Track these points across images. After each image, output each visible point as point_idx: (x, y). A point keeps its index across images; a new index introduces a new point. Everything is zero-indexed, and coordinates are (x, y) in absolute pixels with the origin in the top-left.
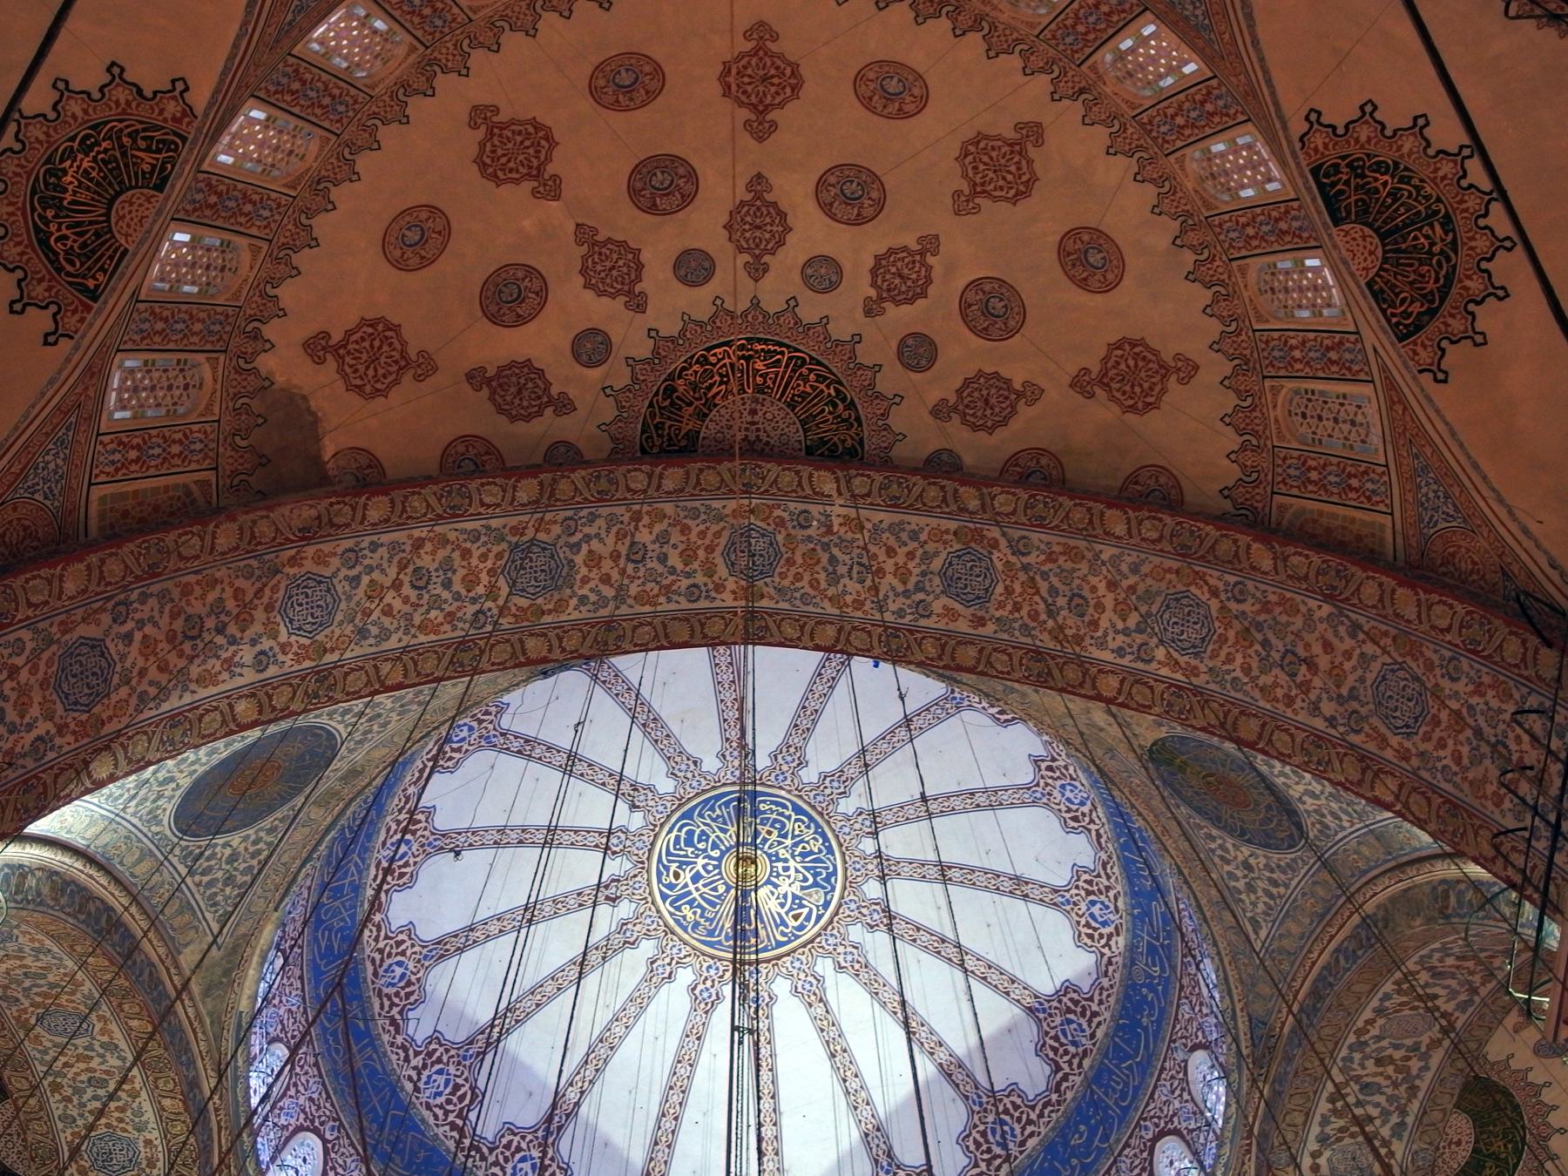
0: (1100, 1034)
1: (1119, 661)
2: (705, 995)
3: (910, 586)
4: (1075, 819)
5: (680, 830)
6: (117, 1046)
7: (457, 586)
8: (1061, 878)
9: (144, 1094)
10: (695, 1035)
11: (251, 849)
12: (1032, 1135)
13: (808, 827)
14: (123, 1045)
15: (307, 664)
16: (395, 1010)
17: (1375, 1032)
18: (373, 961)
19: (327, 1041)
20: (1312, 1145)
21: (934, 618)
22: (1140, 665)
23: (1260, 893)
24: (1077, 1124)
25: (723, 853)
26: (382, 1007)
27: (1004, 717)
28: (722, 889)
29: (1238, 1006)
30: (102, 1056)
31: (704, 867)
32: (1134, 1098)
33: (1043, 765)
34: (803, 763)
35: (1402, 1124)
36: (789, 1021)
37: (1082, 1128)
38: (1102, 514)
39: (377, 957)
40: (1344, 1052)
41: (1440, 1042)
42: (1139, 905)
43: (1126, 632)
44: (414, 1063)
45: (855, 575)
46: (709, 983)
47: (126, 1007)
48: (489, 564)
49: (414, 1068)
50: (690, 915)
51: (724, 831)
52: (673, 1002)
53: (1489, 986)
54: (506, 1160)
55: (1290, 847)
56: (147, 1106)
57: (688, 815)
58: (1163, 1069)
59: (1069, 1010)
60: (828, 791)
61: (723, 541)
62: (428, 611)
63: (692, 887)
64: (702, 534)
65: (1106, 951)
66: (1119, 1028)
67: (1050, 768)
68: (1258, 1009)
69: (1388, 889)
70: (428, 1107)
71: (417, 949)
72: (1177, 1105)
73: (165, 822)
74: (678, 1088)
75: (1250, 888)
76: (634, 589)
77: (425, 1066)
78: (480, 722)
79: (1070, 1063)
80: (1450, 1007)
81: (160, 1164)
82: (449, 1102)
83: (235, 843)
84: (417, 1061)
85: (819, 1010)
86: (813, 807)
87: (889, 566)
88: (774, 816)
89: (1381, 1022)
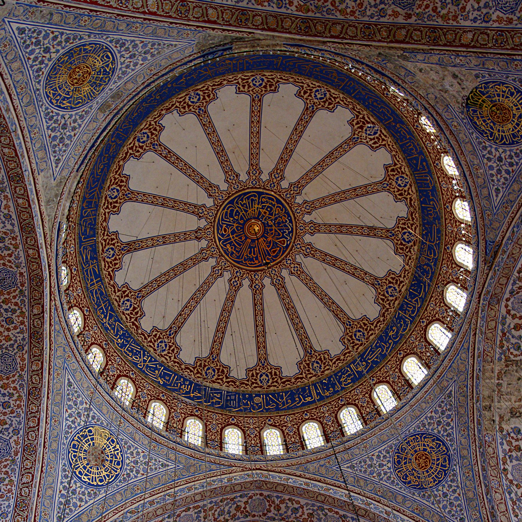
2: (235, 284)
5: (228, 209)
10: (231, 300)
13: (282, 210)
16: (110, 270)
18: (102, 244)
19: (84, 274)
25: (245, 222)
26: (105, 266)
28: (243, 238)
31: (237, 227)
36: (270, 294)
39: (104, 243)
44: (117, 294)
46: (237, 279)
49: (118, 296)
54: (155, 341)
57: (231, 202)
60: (292, 192)
63: (231, 236)
70: (123, 313)
71: (119, 244)
73: (42, 83)
77: (122, 297)
82: (132, 313)
86: (285, 200)
88: (268, 205)
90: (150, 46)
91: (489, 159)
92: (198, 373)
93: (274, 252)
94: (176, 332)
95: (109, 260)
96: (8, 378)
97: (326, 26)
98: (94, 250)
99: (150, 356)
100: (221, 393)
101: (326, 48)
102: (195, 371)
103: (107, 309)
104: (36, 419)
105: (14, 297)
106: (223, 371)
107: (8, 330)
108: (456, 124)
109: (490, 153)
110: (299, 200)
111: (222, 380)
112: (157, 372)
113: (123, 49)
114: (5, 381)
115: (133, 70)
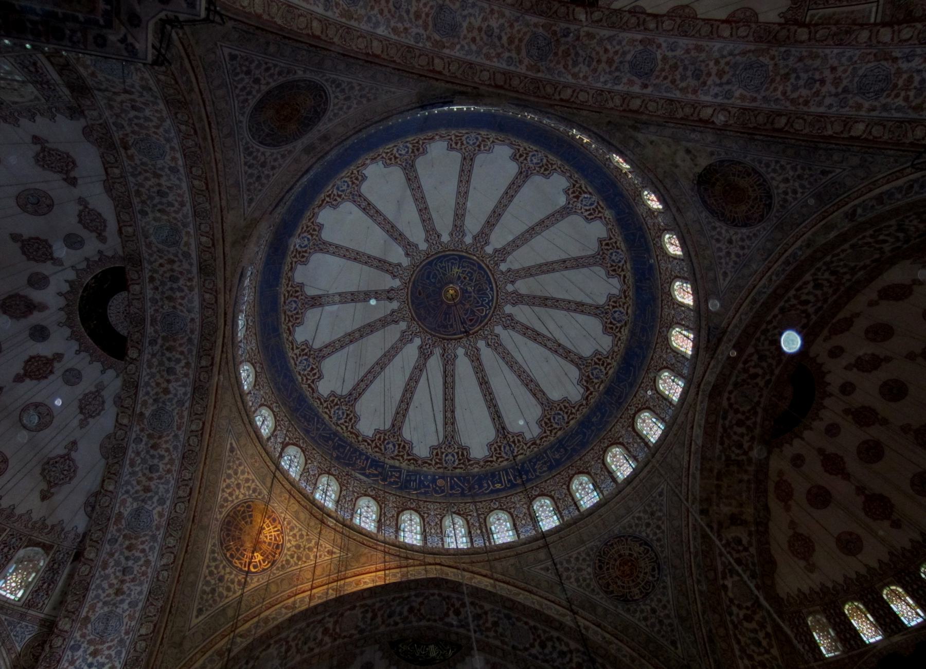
0: (610, 372)
1: (714, 100)
3: (613, 68)
4: (614, 270)
6: (190, 255)
7: (412, 16)
8: (602, 301)
9: (196, 290)
11: (272, 163)
14: (194, 255)
15: (344, 20)
16: (290, 324)
17: (775, 323)
20: (730, 388)
21: (622, 85)
22: (726, 101)
23: (733, 256)
27: (590, 217)
30: (181, 261)
33: (604, 243)
34: (487, 243)
36: (463, 366)
37: (598, 413)
38: (718, 27)
40: (758, 334)
43: (721, 85)
45: (586, 62)
47: (203, 227)
48: (427, 10)
51: (444, 274)
52: (411, 352)
53: (835, 297)
55: (760, 221)
56: (196, 298)
57: (430, 263)
58: (642, 382)
61: (527, 38)
62: (397, 22)
64: (519, 31)
65: (619, 334)
67: (607, 244)
76: (484, 51)
78: (353, 183)
80: (811, 310)
81: (196, 333)
82: (308, 375)
83: (268, 154)
84: (297, 351)
87: (604, 58)
88: (469, 270)
89: (780, 316)
90: (367, 90)
91: (718, 241)
92: (376, 446)
93: (471, 320)
97: (556, 89)
100: (400, 472)
101: (553, 111)
102: (374, 445)
104: (188, 488)
106: (404, 447)
108: (684, 201)
109: (720, 234)
110: (503, 267)
111: (402, 456)
112: (330, 442)
113: (338, 90)
115: (346, 113)
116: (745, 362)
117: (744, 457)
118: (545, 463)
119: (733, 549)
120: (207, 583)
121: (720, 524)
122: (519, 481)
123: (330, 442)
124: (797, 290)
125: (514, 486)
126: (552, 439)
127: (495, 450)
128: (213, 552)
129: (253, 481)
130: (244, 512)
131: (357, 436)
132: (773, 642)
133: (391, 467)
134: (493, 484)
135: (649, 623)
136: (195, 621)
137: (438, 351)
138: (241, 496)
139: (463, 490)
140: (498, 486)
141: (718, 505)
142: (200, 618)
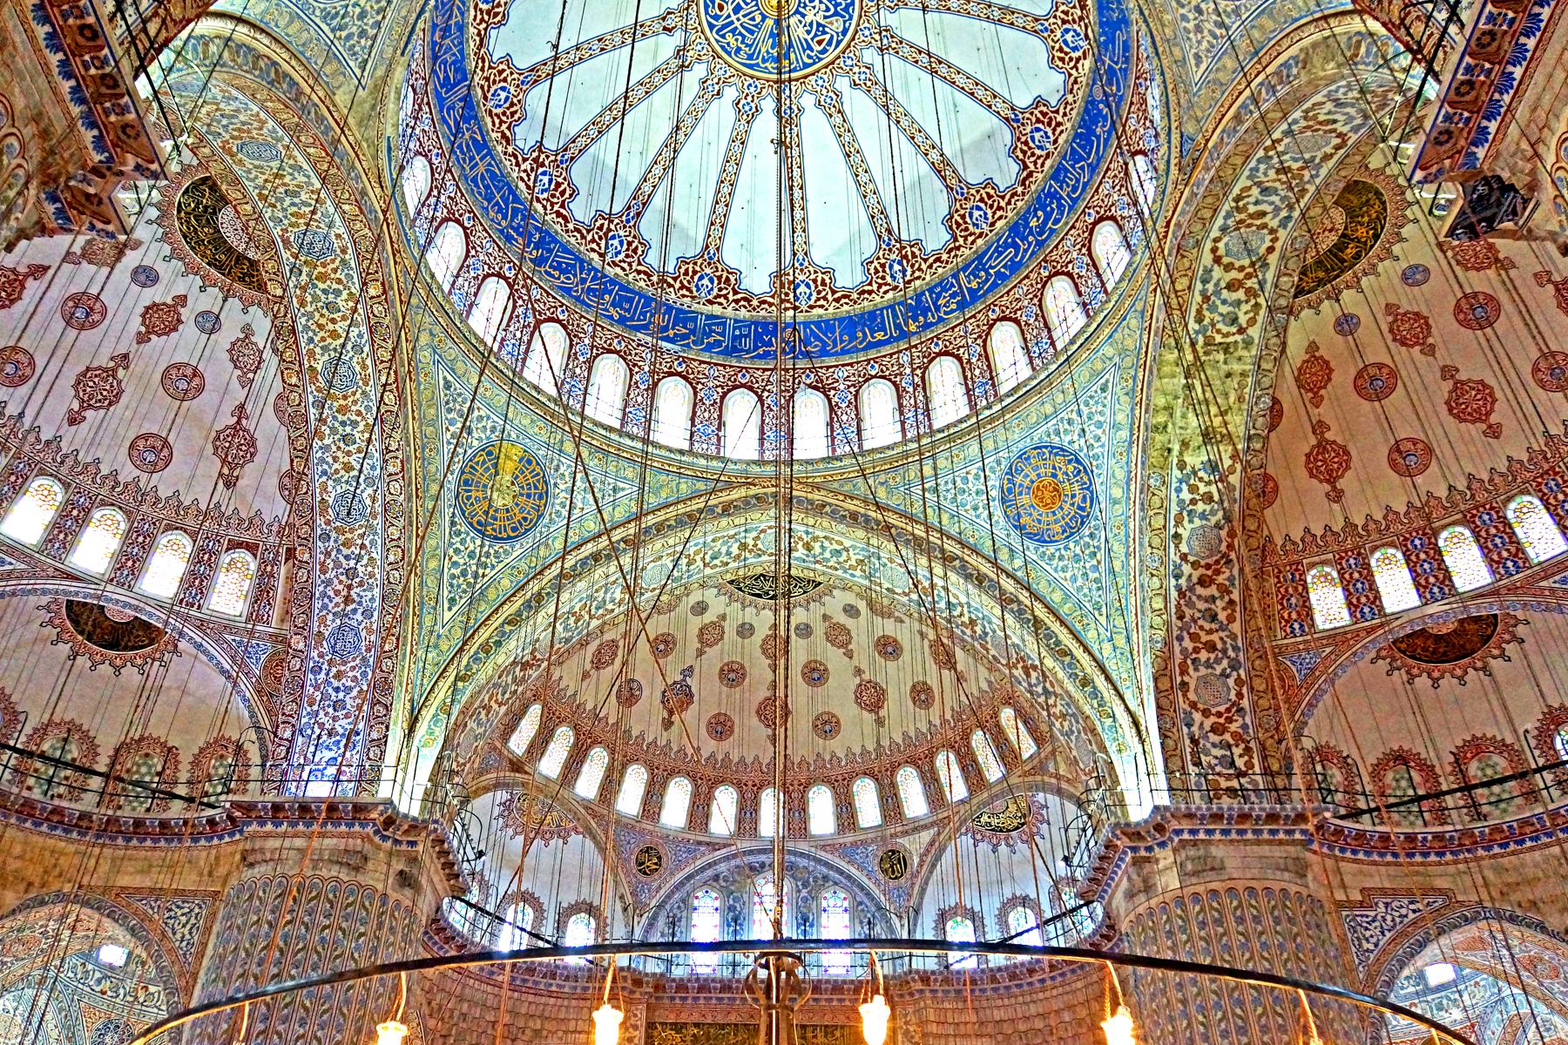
12: (1000, 218)
16: (504, 126)
20: (1215, 233)
23: (1206, 32)
24: (1036, 210)
28: (758, 19)
29: (1174, 125)
32: (1083, 190)
35: (1289, 218)
36: (814, 127)
37: (1040, 213)
40: (1253, 164)
41: (1332, 155)
42: (1104, 34)
44: (523, 167)
50: (732, 41)
52: (721, 115)
59: (1038, 121)
63: (733, 17)
65: (1073, 72)
66: (1077, 135)
68: (1190, 128)
69: (1314, 36)
72: (1116, 197)
74: (727, 182)
75: (1198, 29)
79: (1035, 163)
80: (1345, 129)
82: (553, 196)
85: (838, 119)
92: (683, 287)
94: (638, 214)
95: (499, 111)
96: (345, 398)
98: (467, 100)
99: (594, 268)
102: (677, 285)
103: (506, 201)
105: (335, 270)
106: (728, 279)
107: (333, 321)
111: (725, 297)
112: (607, 297)
114: (342, 402)
116: (1238, 199)
117: (1238, 338)
118: (953, 296)
119: (1201, 479)
120: (455, 564)
121: (1185, 444)
122: (913, 328)
123: (607, 297)
124: (1306, 112)
125: (905, 335)
126: (967, 252)
127: (877, 271)
128: (453, 523)
129: (488, 418)
130: (484, 462)
131: (649, 276)
132: (1238, 615)
133: (709, 317)
134: (873, 332)
135: (1068, 575)
136: (448, 615)
137: (769, 105)
138: (475, 443)
139: (825, 344)
140: (879, 336)
141: (1184, 416)
142: (455, 609)
